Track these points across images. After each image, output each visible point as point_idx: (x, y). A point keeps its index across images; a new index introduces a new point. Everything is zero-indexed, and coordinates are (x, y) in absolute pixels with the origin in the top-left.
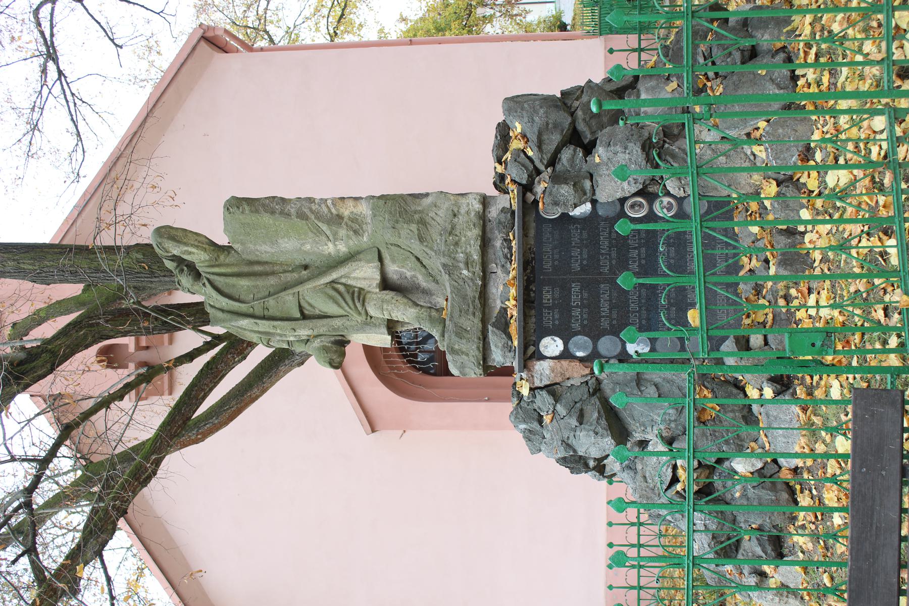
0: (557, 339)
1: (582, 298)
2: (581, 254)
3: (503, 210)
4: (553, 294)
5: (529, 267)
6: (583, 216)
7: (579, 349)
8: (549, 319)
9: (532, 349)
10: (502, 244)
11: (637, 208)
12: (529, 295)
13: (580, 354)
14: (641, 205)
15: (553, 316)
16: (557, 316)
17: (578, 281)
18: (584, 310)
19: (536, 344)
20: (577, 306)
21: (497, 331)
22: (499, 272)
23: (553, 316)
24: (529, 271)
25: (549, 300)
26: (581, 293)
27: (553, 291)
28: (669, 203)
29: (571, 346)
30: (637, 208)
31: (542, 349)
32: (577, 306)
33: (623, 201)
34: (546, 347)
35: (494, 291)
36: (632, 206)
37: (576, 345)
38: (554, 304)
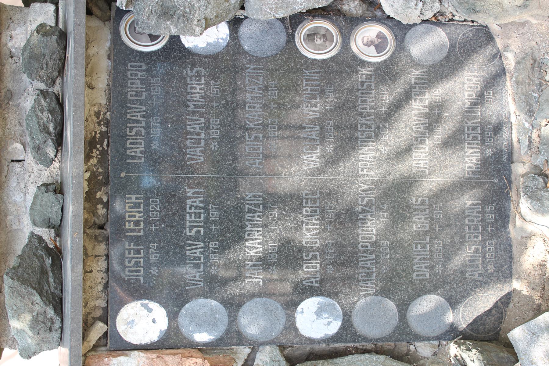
0: (153, 305)
1: (207, 220)
2: (207, 128)
3: (41, 29)
4: (146, 211)
5: (95, 153)
6: (212, 51)
7: (200, 327)
8: (137, 264)
9: (99, 329)
10: (37, 101)
11: (319, 41)
12: (94, 212)
13: (202, 337)
14: (327, 36)
15: (147, 258)
16: (154, 258)
17: (200, 184)
18: (212, 245)
19: (107, 316)
20: (197, 238)
21: (24, 290)
22: (29, 159)
23: (147, 258)
24: (94, 161)
25: (137, 223)
26: (206, 210)
27: (147, 205)
28: (380, 36)
29: (183, 320)
30: (319, 41)
31: (121, 327)
32: (197, 238)
33: (295, 20)
34: (130, 324)
35: (17, 197)
36: (311, 36)
37: (193, 317)
38: (148, 232)
